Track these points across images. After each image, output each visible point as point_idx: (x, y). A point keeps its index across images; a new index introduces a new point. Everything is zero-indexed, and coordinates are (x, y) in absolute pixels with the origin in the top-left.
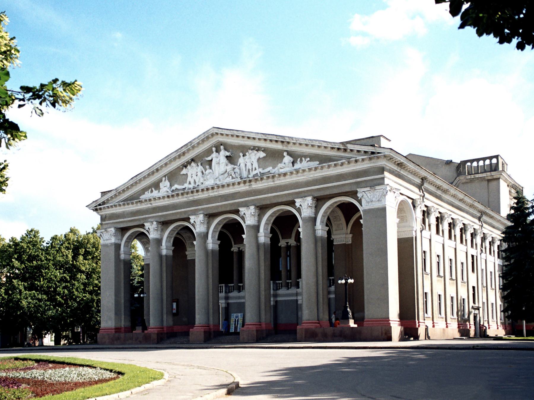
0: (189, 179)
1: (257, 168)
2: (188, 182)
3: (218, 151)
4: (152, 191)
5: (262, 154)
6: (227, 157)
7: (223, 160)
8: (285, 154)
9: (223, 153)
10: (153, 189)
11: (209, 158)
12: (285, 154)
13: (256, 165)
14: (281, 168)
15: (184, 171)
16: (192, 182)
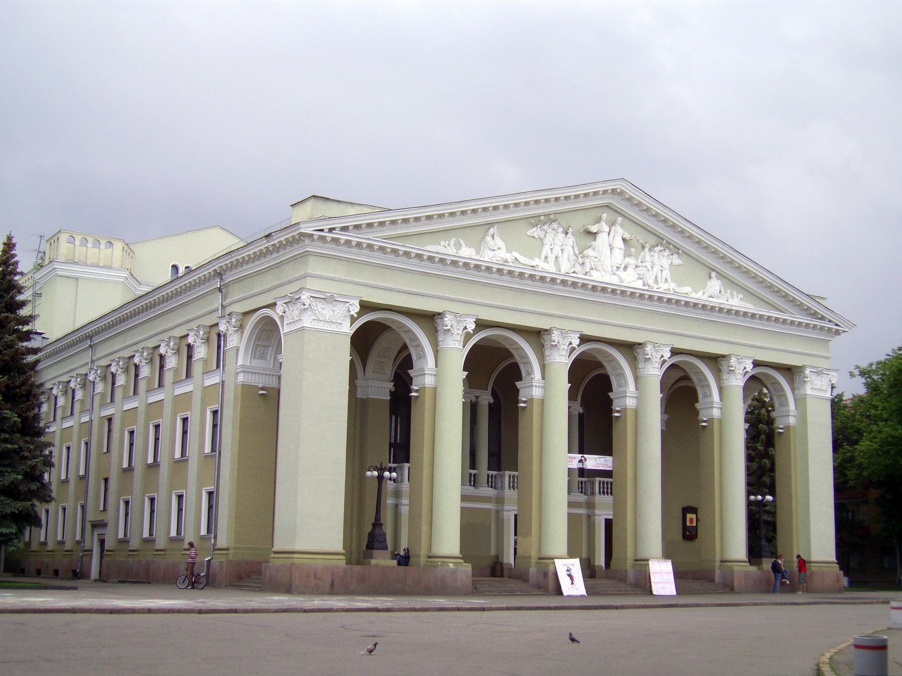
0: (546, 250)
1: (669, 280)
2: (543, 258)
3: (612, 224)
4: (458, 246)
5: (676, 260)
6: (624, 240)
7: (619, 243)
8: (714, 274)
9: (619, 232)
10: (462, 242)
11: (594, 229)
12: (714, 274)
13: (666, 274)
14: (711, 297)
15: (535, 232)
16: (552, 259)
